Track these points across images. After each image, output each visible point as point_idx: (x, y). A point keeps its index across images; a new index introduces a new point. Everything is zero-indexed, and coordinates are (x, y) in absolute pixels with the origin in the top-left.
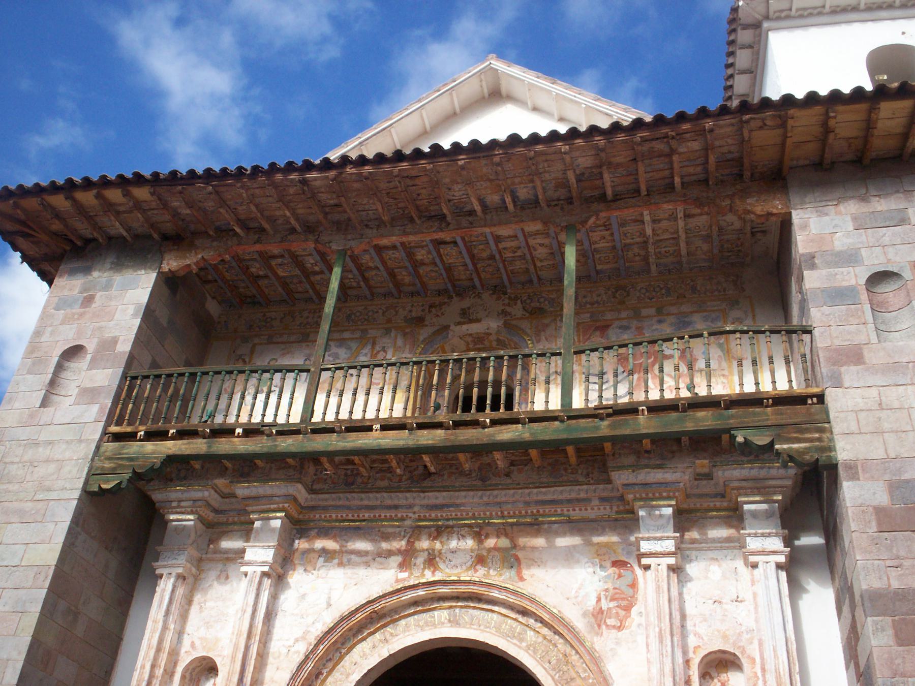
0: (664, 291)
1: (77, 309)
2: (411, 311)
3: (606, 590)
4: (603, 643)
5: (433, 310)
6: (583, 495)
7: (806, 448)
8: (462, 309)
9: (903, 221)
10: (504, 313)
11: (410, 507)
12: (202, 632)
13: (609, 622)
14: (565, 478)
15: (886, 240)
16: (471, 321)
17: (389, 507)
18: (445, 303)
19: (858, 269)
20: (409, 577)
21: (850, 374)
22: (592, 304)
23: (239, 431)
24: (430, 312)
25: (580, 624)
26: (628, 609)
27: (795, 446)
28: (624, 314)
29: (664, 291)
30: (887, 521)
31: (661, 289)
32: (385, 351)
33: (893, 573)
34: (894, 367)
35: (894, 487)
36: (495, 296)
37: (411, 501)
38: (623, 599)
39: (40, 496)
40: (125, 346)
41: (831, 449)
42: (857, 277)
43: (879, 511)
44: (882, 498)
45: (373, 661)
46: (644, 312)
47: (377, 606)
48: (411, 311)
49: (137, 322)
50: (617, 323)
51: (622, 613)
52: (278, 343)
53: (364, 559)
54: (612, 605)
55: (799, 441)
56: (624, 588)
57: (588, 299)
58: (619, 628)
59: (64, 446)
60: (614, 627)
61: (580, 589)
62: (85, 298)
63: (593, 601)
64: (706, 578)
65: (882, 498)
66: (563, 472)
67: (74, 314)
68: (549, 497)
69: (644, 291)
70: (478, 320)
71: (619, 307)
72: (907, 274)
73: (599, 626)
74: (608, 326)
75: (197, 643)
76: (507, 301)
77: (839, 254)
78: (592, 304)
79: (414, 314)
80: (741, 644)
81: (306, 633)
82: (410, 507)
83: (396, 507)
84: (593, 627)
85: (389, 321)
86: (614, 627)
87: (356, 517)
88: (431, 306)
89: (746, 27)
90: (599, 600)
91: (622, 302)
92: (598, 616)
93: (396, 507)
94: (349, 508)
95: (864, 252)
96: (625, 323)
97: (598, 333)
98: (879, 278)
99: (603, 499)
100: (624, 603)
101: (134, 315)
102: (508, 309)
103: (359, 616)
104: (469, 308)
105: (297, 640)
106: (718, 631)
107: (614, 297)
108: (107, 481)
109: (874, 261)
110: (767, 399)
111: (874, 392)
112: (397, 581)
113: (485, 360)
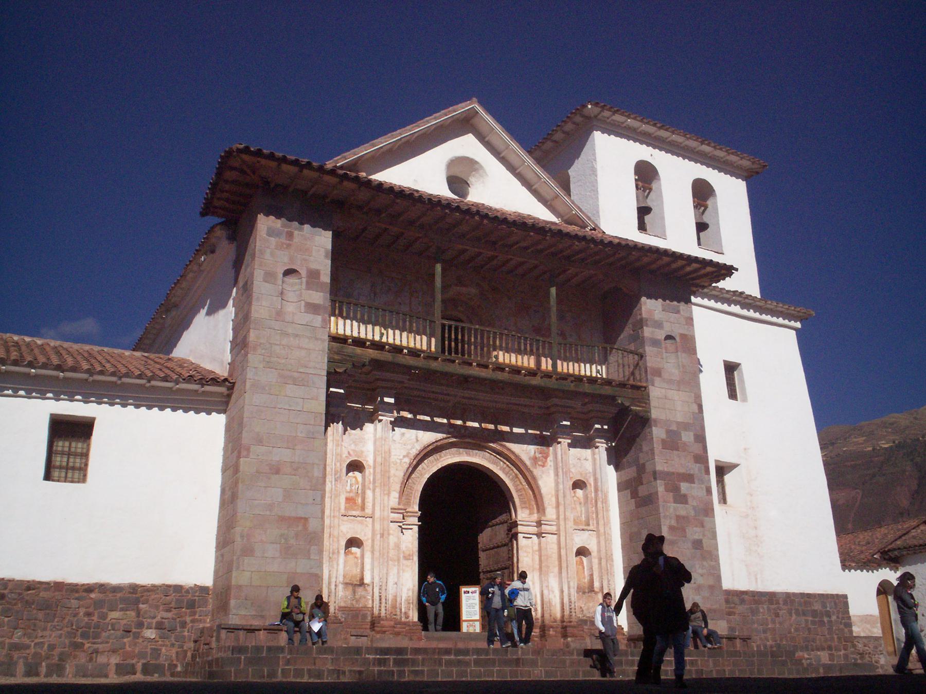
1: (283, 240)
4: (537, 472)
9: (678, 312)
12: (353, 447)
15: (672, 320)
19: (663, 332)
21: (657, 380)
23: (405, 351)
25: (528, 463)
26: (546, 458)
30: (666, 445)
33: (665, 465)
34: (670, 382)
35: (668, 432)
39: (301, 370)
40: (326, 278)
41: (650, 412)
42: (660, 335)
43: (663, 440)
44: (664, 436)
45: (435, 469)
47: (439, 444)
49: (329, 262)
58: (543, 466)
59: (307, 340)
62: (287, 232)
65: (664, 436)
67: (283, 244)
72: (678, 339)
75: (351, 453)
77: (656, 322)
83: (448, 395)
89: (583, 116)
95: (665, 323)
98: (669, 337)
99: (540, 407)
101: (326, 257)
103: (431, 447)
105: (404, 457)
108: (339, 367)
109: (668, 329)
111: (663, 391)
113: (520, 338)
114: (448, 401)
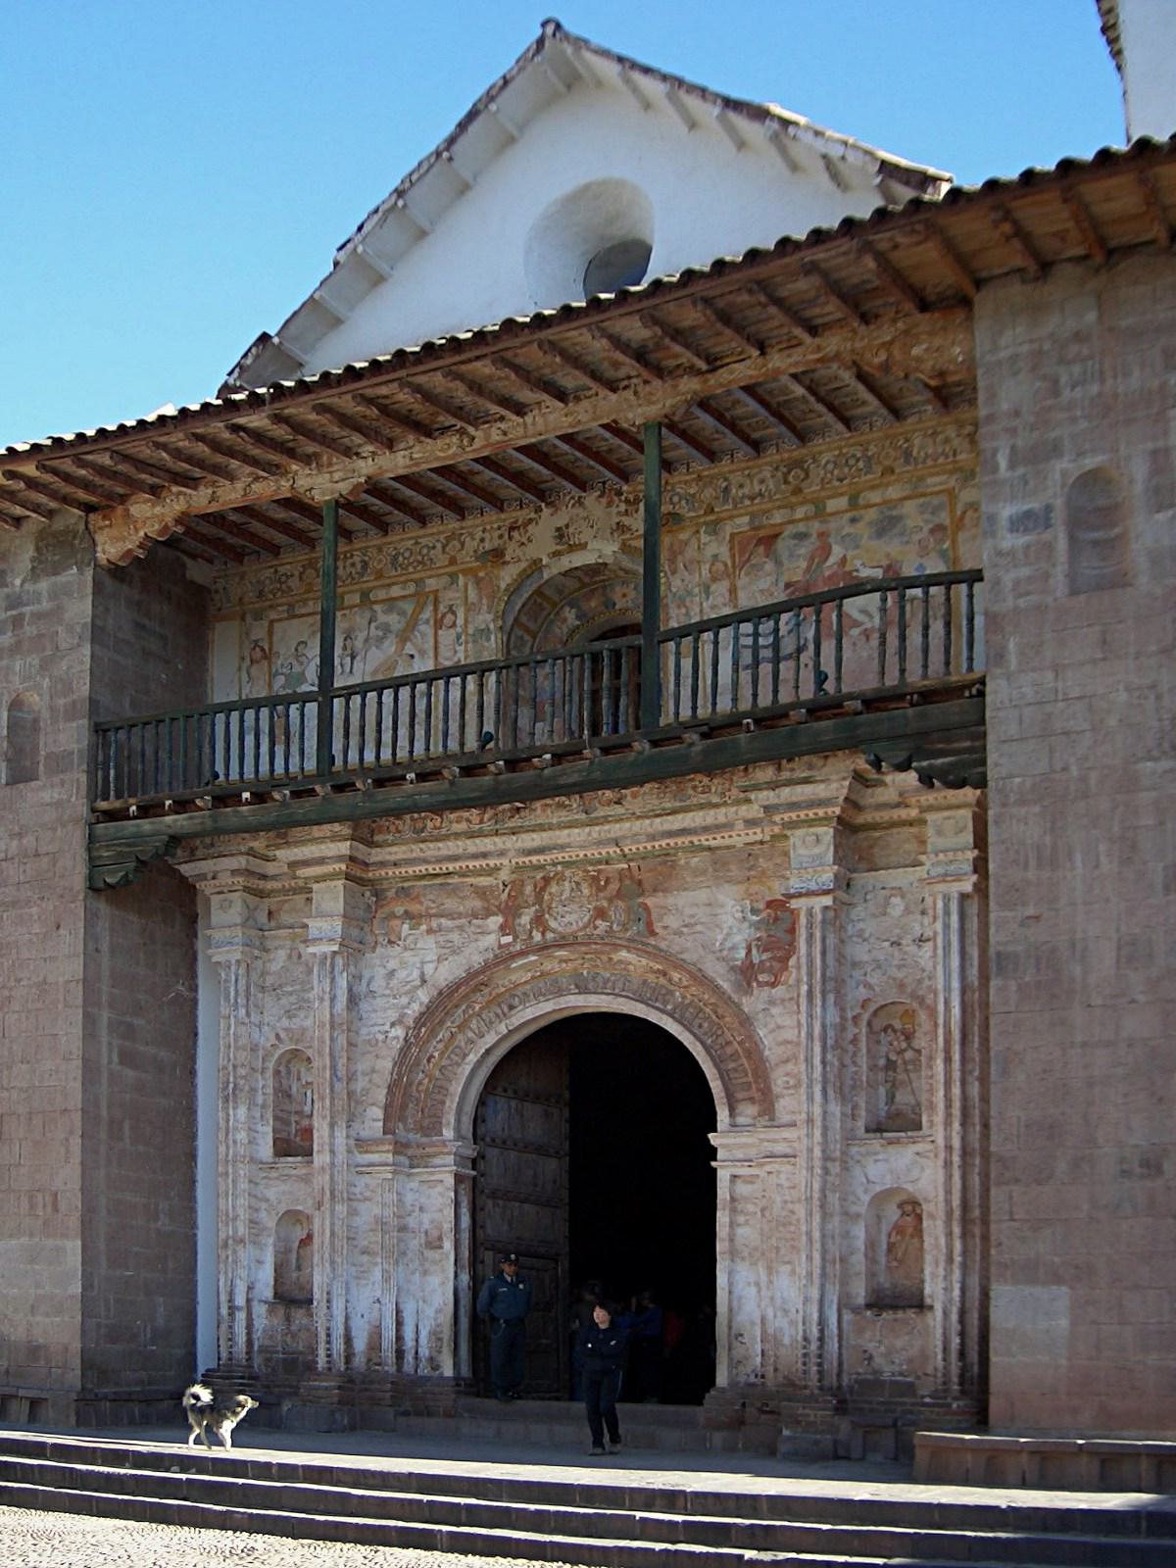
0: (861, 464)
2: (482, 540)
3: (759, 939)
5: (515, 534)
6: (722, 819)
7: (951, 764)
8: (558, 529)
10: (621, 528)
11: (502, 853)
13: (762, 978)
14: (695, 801)
16: (573, 548)
17: (475, 857)
18: (531, 521)
20: (514, 940)
22: (752, 498)
24: (510, 538)
26: (784, 960)
27: (940, 761)
28: (800, 513)
29: (861, 464)
31: (858, 460)
32: (454, 613)
36: (604, 501)
37: (500, 846)
38: (779, 949)
46: (832, 505)
48: (482, 540)
50: (790, 530)
51: (777, 965)
52: (303, 616)
53: (458, 922)
54: (765, 956)
55: (943, 753)
56: (781, 934)
57: (746, 490)
58: (773, 985)
60: (767, 984)
61: (725, 940)
63: (742, 954)
64: (884, 914)
66: (691, 792)
68: (676, 826)
69: (830, 467)
70: (583, 546)
71: (793, 499)
73: (749, 984)
74: (776, 536)
76: (623, 507)
78: (752, 498)
79: (488, 546)
80: (921, 993)
81: (403, 1015)
82: (502, 853)
83: (484, 855)
84: (740, 985)
85: (453, 561)
86: (767, 984)
87: (438, 871)
88: (512, 529)
90: (749, 951)
91: (798, 491)
92: (747, 974)
93: (484, 855)
94: (425, 861)
96: (801, 528)
97: (761, 549)
100: (779, 954)
102: (626, 521)
104: (567, 526)
106: (894, 979)
107: (786, 482)
110: (912, 694)
112: (500, 946)
114: (497, 869)
